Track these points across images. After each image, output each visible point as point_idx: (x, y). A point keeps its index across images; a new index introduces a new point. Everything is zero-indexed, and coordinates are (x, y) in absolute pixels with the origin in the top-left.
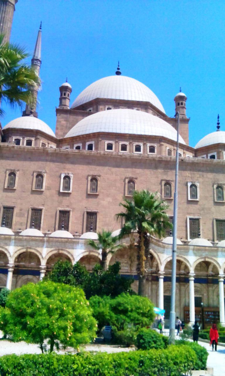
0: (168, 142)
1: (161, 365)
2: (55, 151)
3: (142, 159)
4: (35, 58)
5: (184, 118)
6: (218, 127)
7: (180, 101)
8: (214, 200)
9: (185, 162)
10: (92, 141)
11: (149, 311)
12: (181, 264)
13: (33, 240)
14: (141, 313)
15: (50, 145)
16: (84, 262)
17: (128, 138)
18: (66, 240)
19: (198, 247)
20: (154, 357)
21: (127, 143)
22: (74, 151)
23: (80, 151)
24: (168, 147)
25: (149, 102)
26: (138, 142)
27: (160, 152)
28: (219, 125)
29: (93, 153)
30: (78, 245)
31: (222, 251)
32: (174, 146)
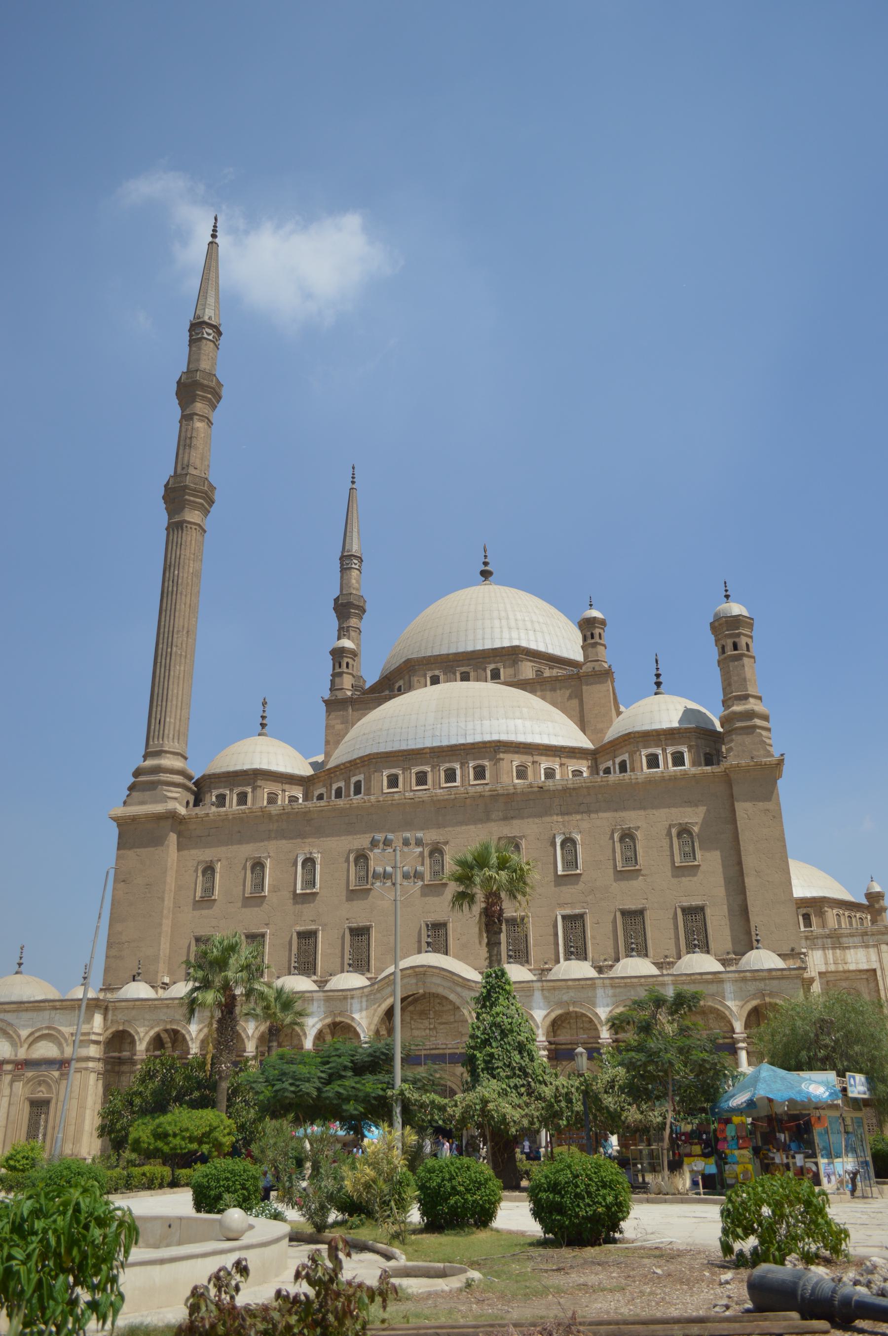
0: (517, 749)
3: (456, 798)
4: (346, 554)
5: (597, 668)
6: (658, 684)
7: (589, 629)
8: (615, 866)
9: (548, 791)
15: (287, 793)
17: (428, 755)
19: (552, 984)
24: (517, 760)
26: (450, 762)
27: (496, 776)
28: (661, 679)
31: (604, 986)
32: (533, 755)
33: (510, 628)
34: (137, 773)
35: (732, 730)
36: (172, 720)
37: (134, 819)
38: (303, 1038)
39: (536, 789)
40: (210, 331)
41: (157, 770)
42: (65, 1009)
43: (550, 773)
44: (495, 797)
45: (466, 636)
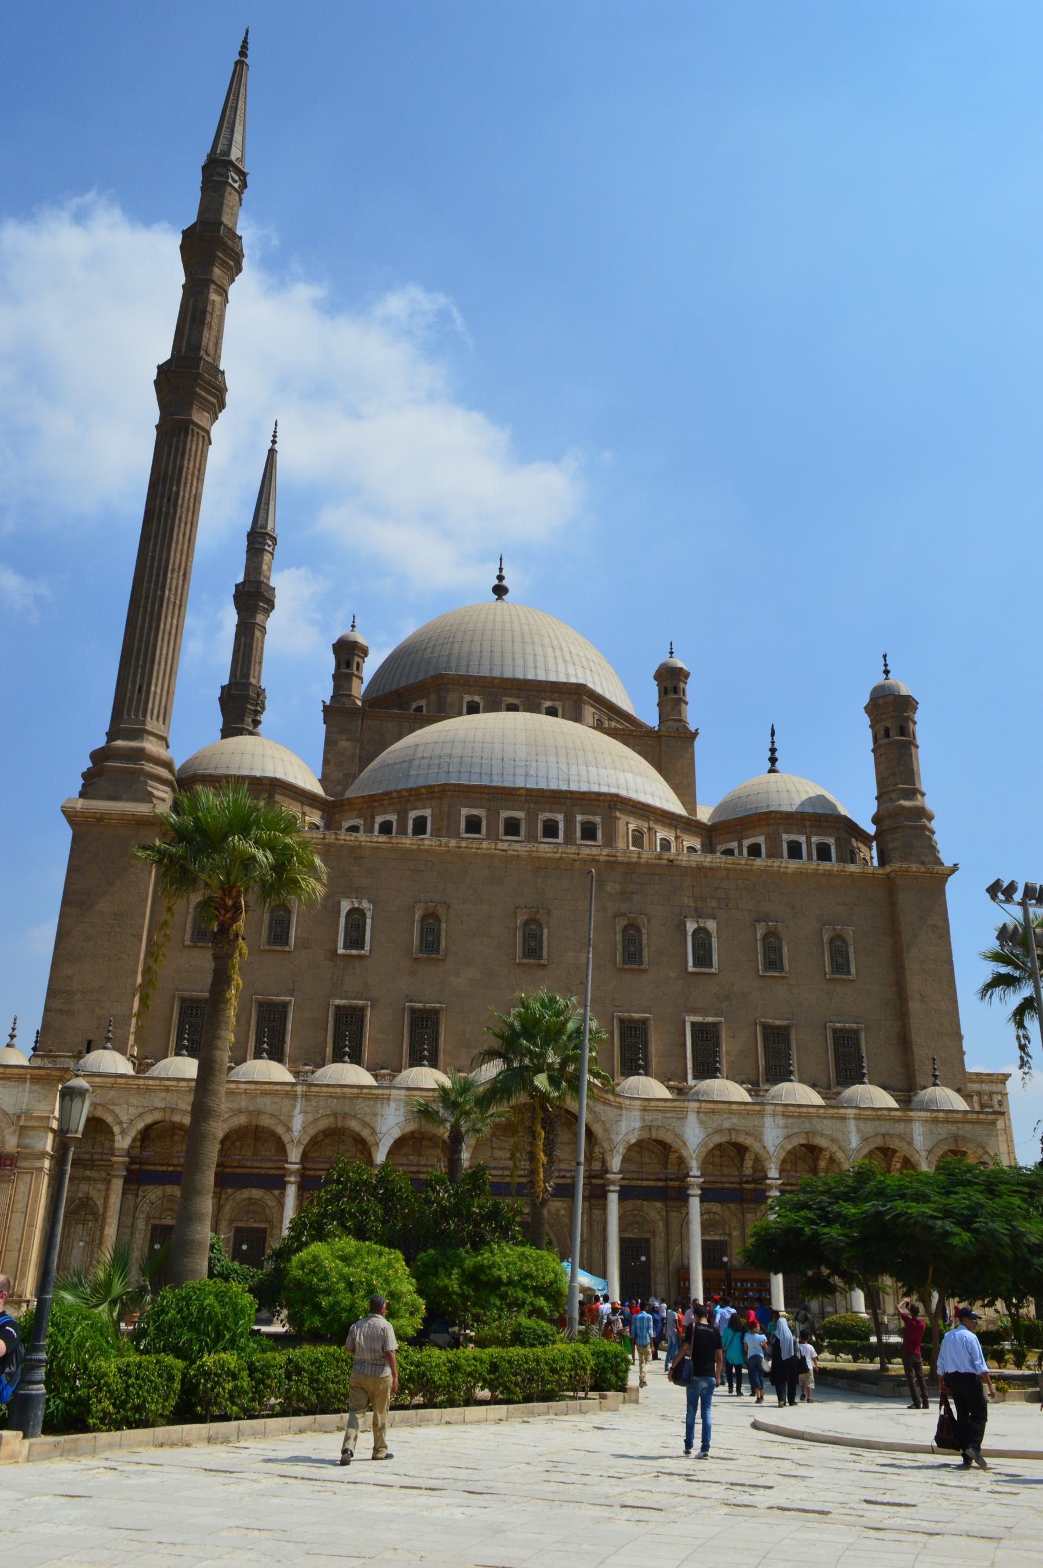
1: (528, 1371)
2: (324, 838)
3: (561, 858)
6: (773, 760)
7: (671, 682)
10: (424, 808)
11: (551, 1283)
12: (669, 1151)
13: (264, 1093)
14: (533, 1287)
16: (405, 1150)
17: (523, 799)
18: (355, 1091)
19: (711, 1106)
20: (516, 1358)
21: (520, 815)
22: (375, 840)
23: (391, 838)
25: (584, 686)
26: (550, 811)
27: (610, 841)
28: (777, 755)
29: (426, 842)
30: (389, 1105)
31: (774, 1115)
33: (565, 661)
34: (98, 756)
35: (898, 827)
36: (159, 691)
37: (101, 818)
38: (373, 1149)
39: (665, 862)
40: (237, 178)
41: (140, 754)
42: (8, 1079)
43: (666, 845)
44: (612, 865)
45: (514, 659)
